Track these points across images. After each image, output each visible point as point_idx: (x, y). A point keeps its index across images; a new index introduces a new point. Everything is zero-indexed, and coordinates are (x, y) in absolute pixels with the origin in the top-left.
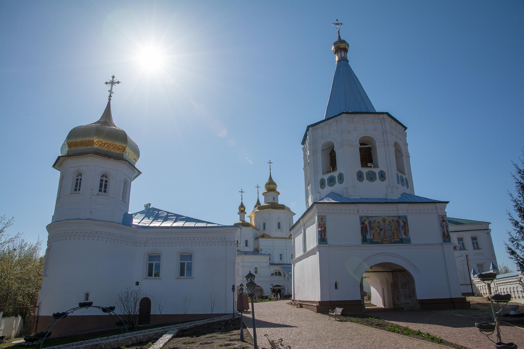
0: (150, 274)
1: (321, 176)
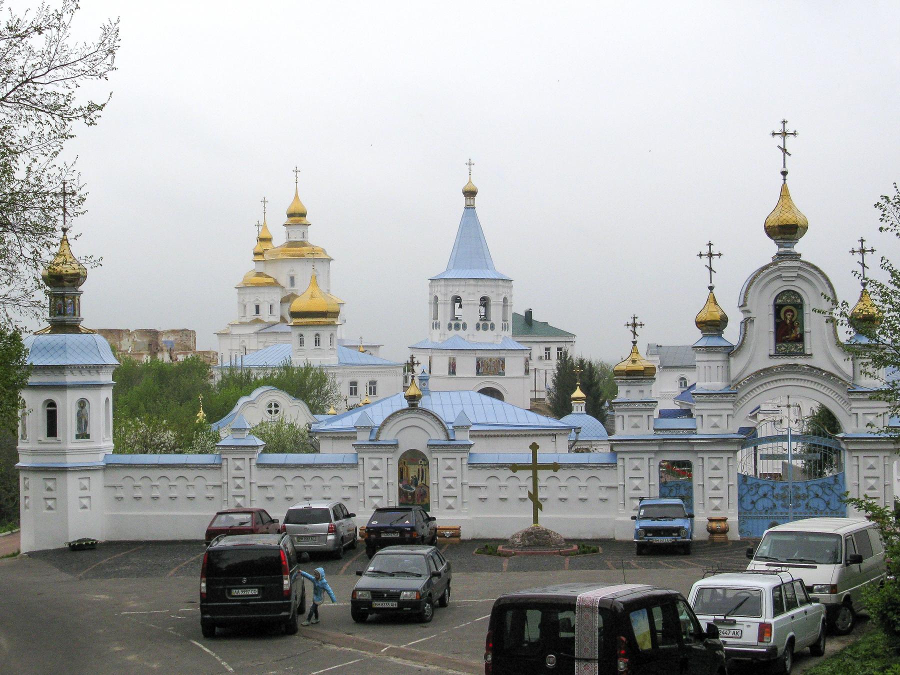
0: (351, 394)
1: (449, 321)
